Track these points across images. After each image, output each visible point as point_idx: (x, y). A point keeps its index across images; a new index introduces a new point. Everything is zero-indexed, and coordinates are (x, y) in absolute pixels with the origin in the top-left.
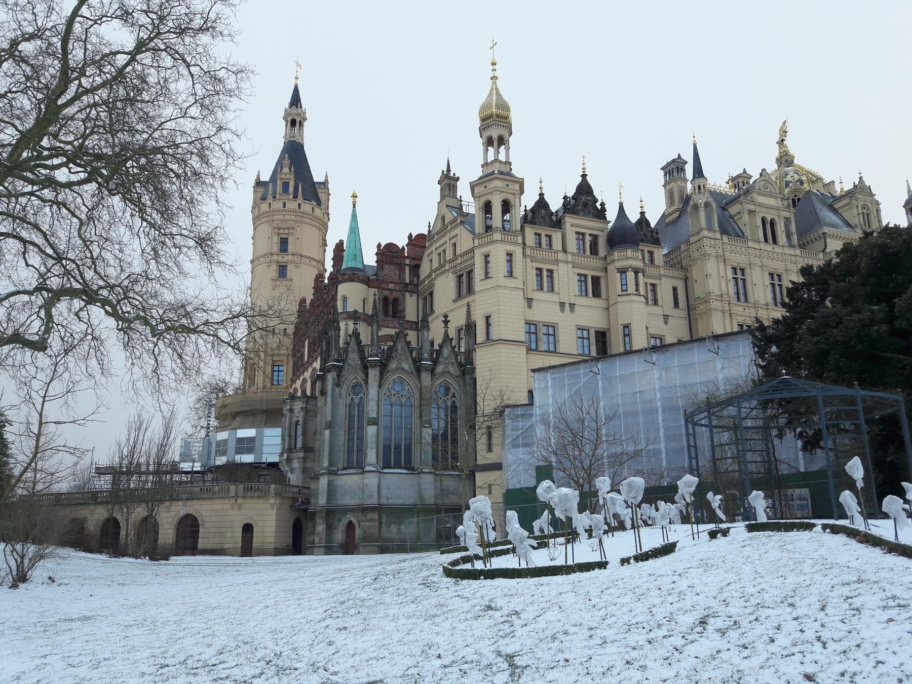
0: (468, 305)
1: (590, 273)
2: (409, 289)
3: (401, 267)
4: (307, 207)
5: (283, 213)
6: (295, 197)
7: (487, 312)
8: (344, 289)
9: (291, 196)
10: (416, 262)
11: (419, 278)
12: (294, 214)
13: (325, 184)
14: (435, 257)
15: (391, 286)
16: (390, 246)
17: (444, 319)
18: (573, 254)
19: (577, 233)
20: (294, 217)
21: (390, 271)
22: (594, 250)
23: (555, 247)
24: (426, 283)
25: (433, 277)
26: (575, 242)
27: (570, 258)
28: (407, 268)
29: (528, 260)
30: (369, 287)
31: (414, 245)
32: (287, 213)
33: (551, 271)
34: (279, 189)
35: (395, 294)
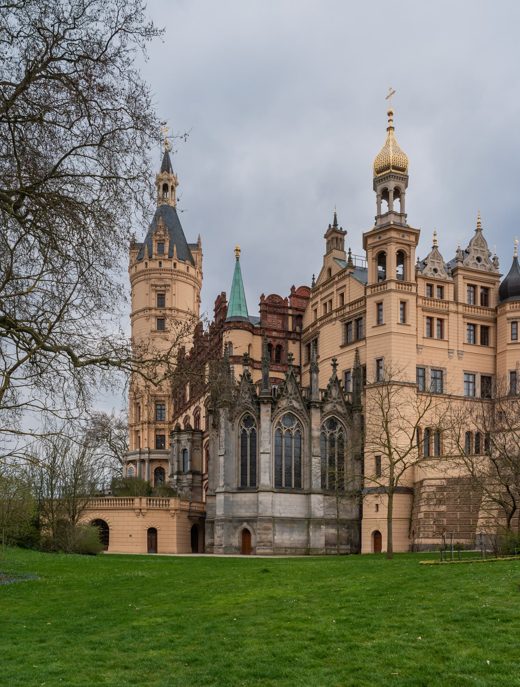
0: (357, 351)
1: (479, 323)
2: (292, 337)
3: (284, 316)
4: (181, 267)
5: (159, 272)
6: (170, 257)
7: (379, 356)
8: (229, 336)
9: (167, 257)
10: (298, 313)
11: (301, 327)
12: (170, 272)
13: (197, 246)
14: (320, 307)
15: (274, 334)
16: (273, 297)
17: (332, 363)
18: (464, 305)
19: (469, 285)
20: (170, 276)
21: (273, 321)
22: (485, 302)
23: (446, 298)
24: (310, 331)
25: (318, 325)
26: (466, 293)
27: (461, 309)
28: (290, 319)
29: (420, 309)
30: (254, 334)
31: (297, 296)
32: (164, 272)
33: (441, 320)
34: (155, 250)
35: (278, 341)
